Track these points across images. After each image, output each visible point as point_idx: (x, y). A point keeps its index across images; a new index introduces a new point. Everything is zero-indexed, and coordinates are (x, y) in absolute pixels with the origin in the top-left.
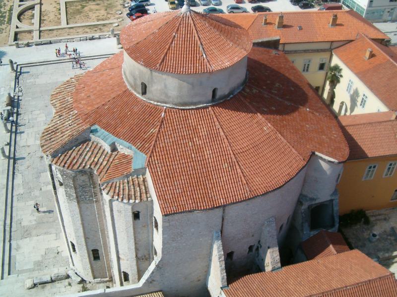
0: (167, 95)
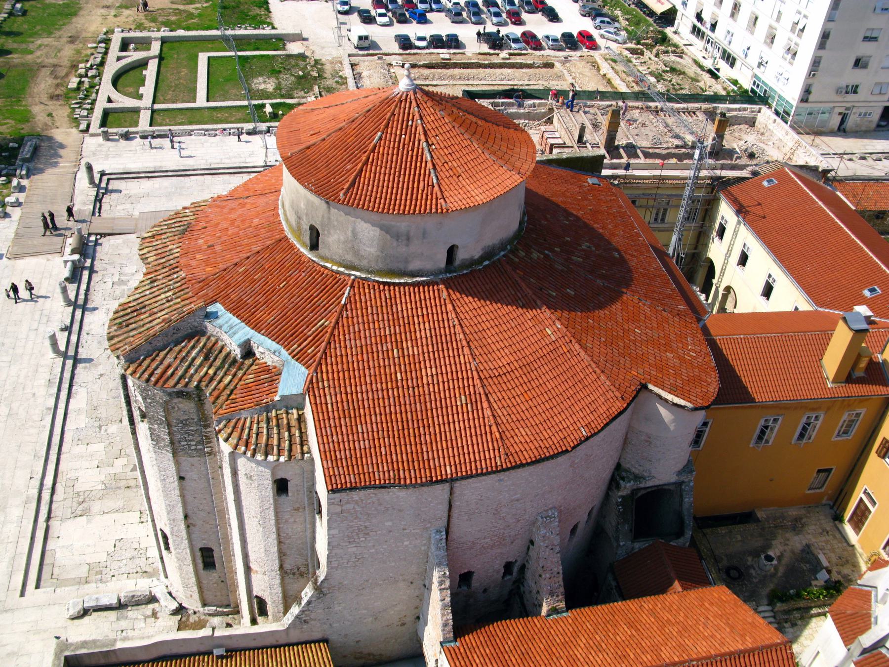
0: (356, 253)
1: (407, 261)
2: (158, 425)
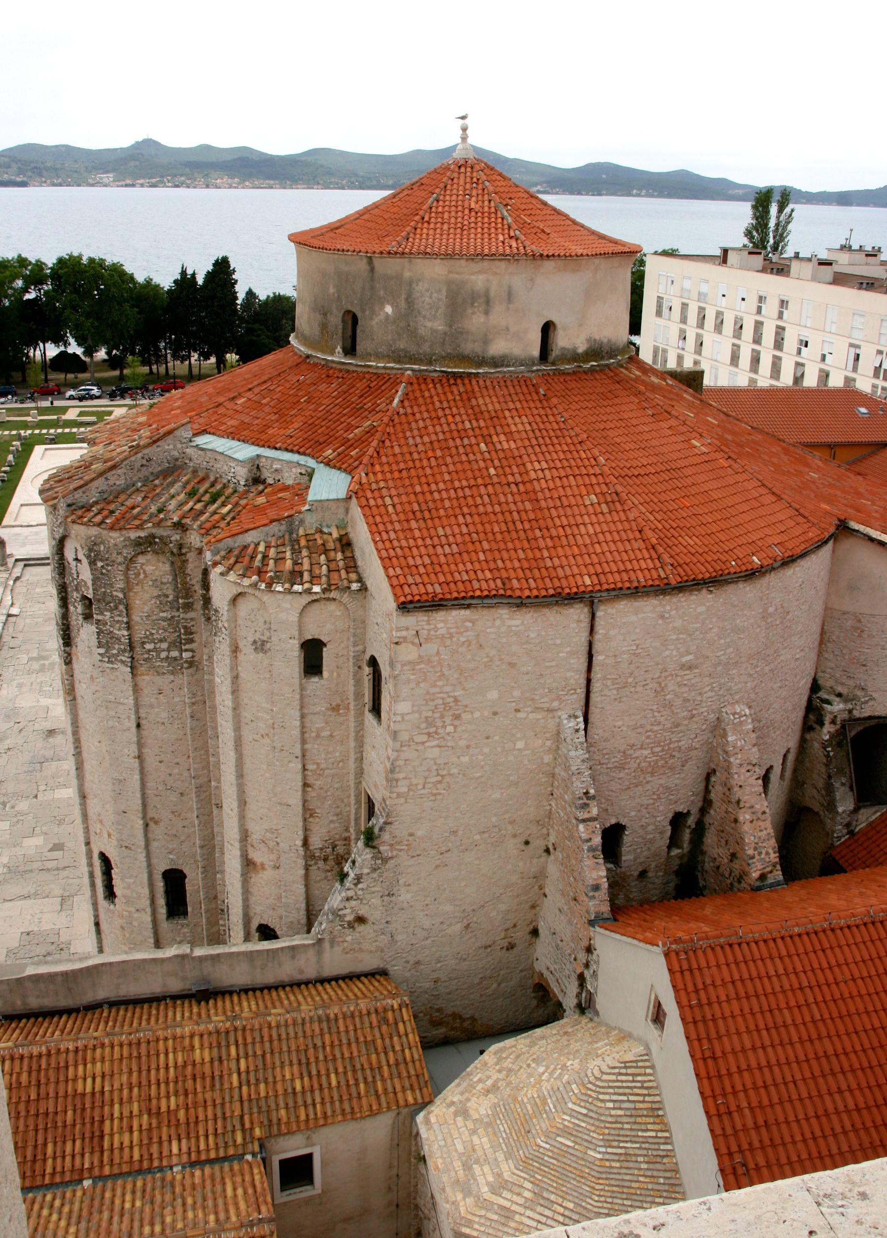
1: (486, 341)
2: (111, 611)
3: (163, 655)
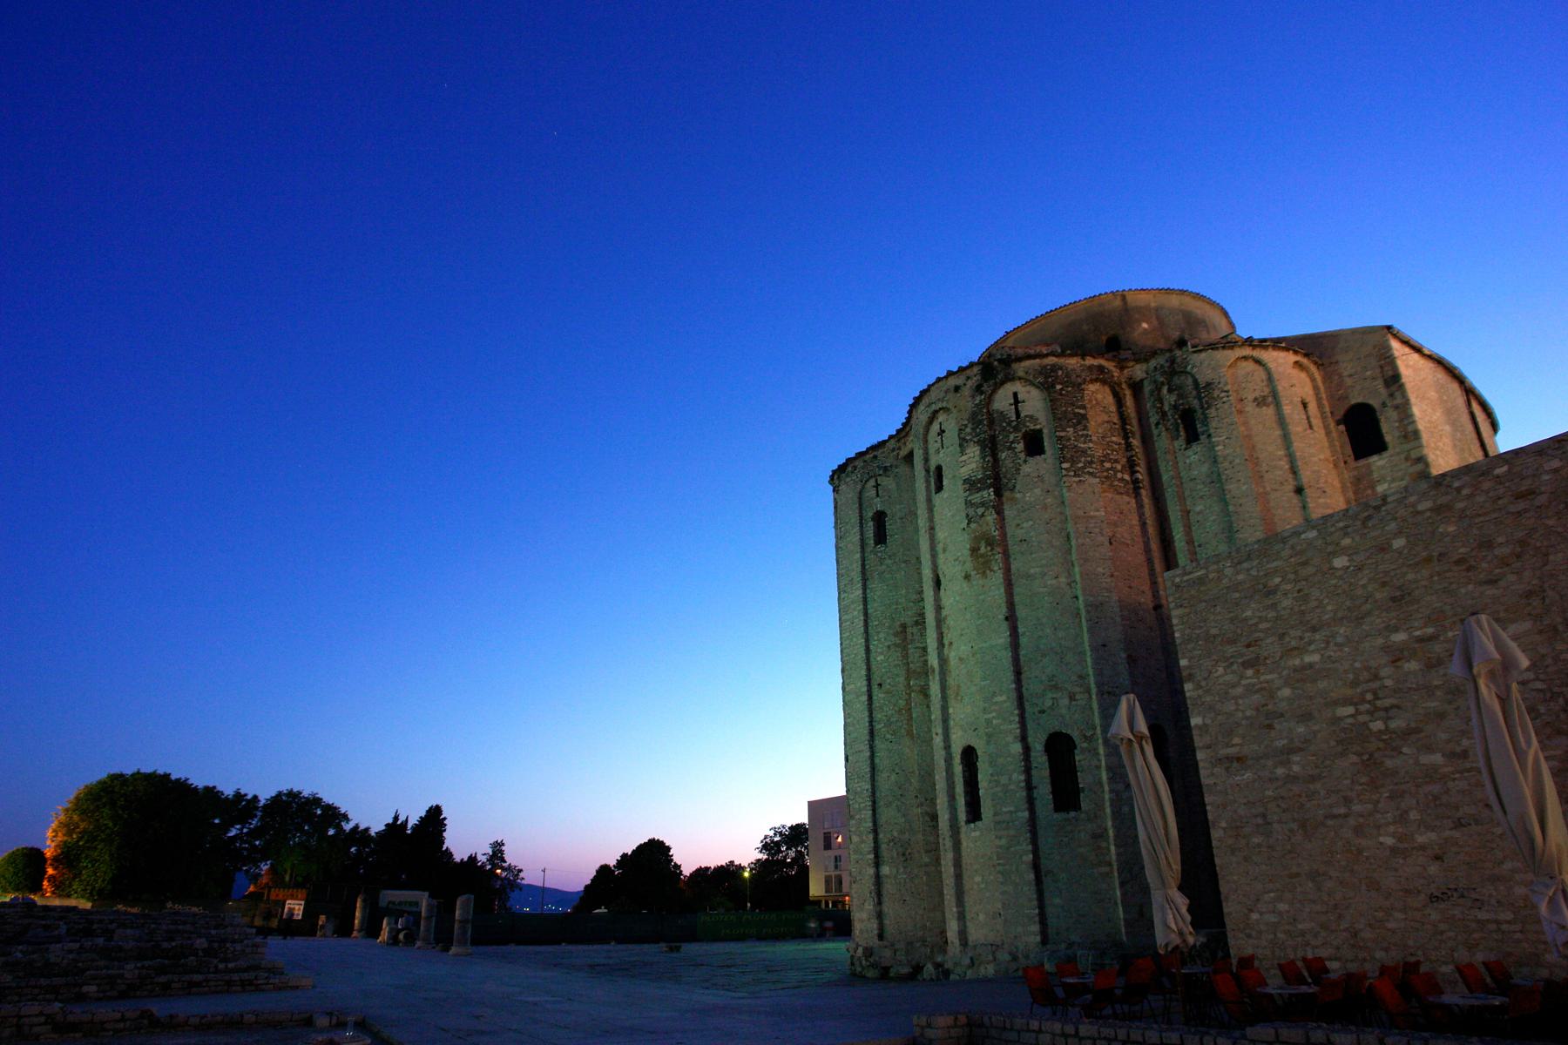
2: (1074, 426)
3: (1119, 475)
